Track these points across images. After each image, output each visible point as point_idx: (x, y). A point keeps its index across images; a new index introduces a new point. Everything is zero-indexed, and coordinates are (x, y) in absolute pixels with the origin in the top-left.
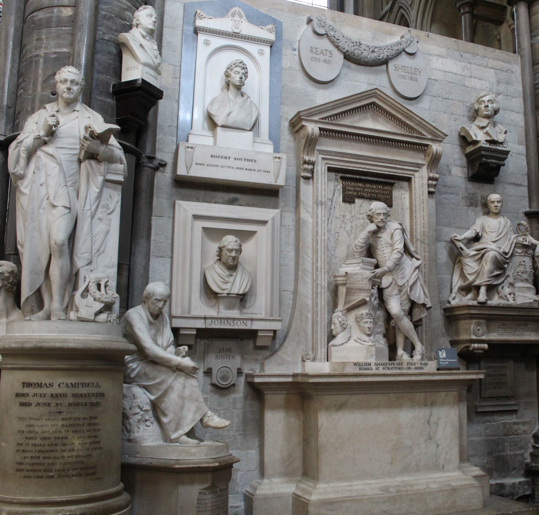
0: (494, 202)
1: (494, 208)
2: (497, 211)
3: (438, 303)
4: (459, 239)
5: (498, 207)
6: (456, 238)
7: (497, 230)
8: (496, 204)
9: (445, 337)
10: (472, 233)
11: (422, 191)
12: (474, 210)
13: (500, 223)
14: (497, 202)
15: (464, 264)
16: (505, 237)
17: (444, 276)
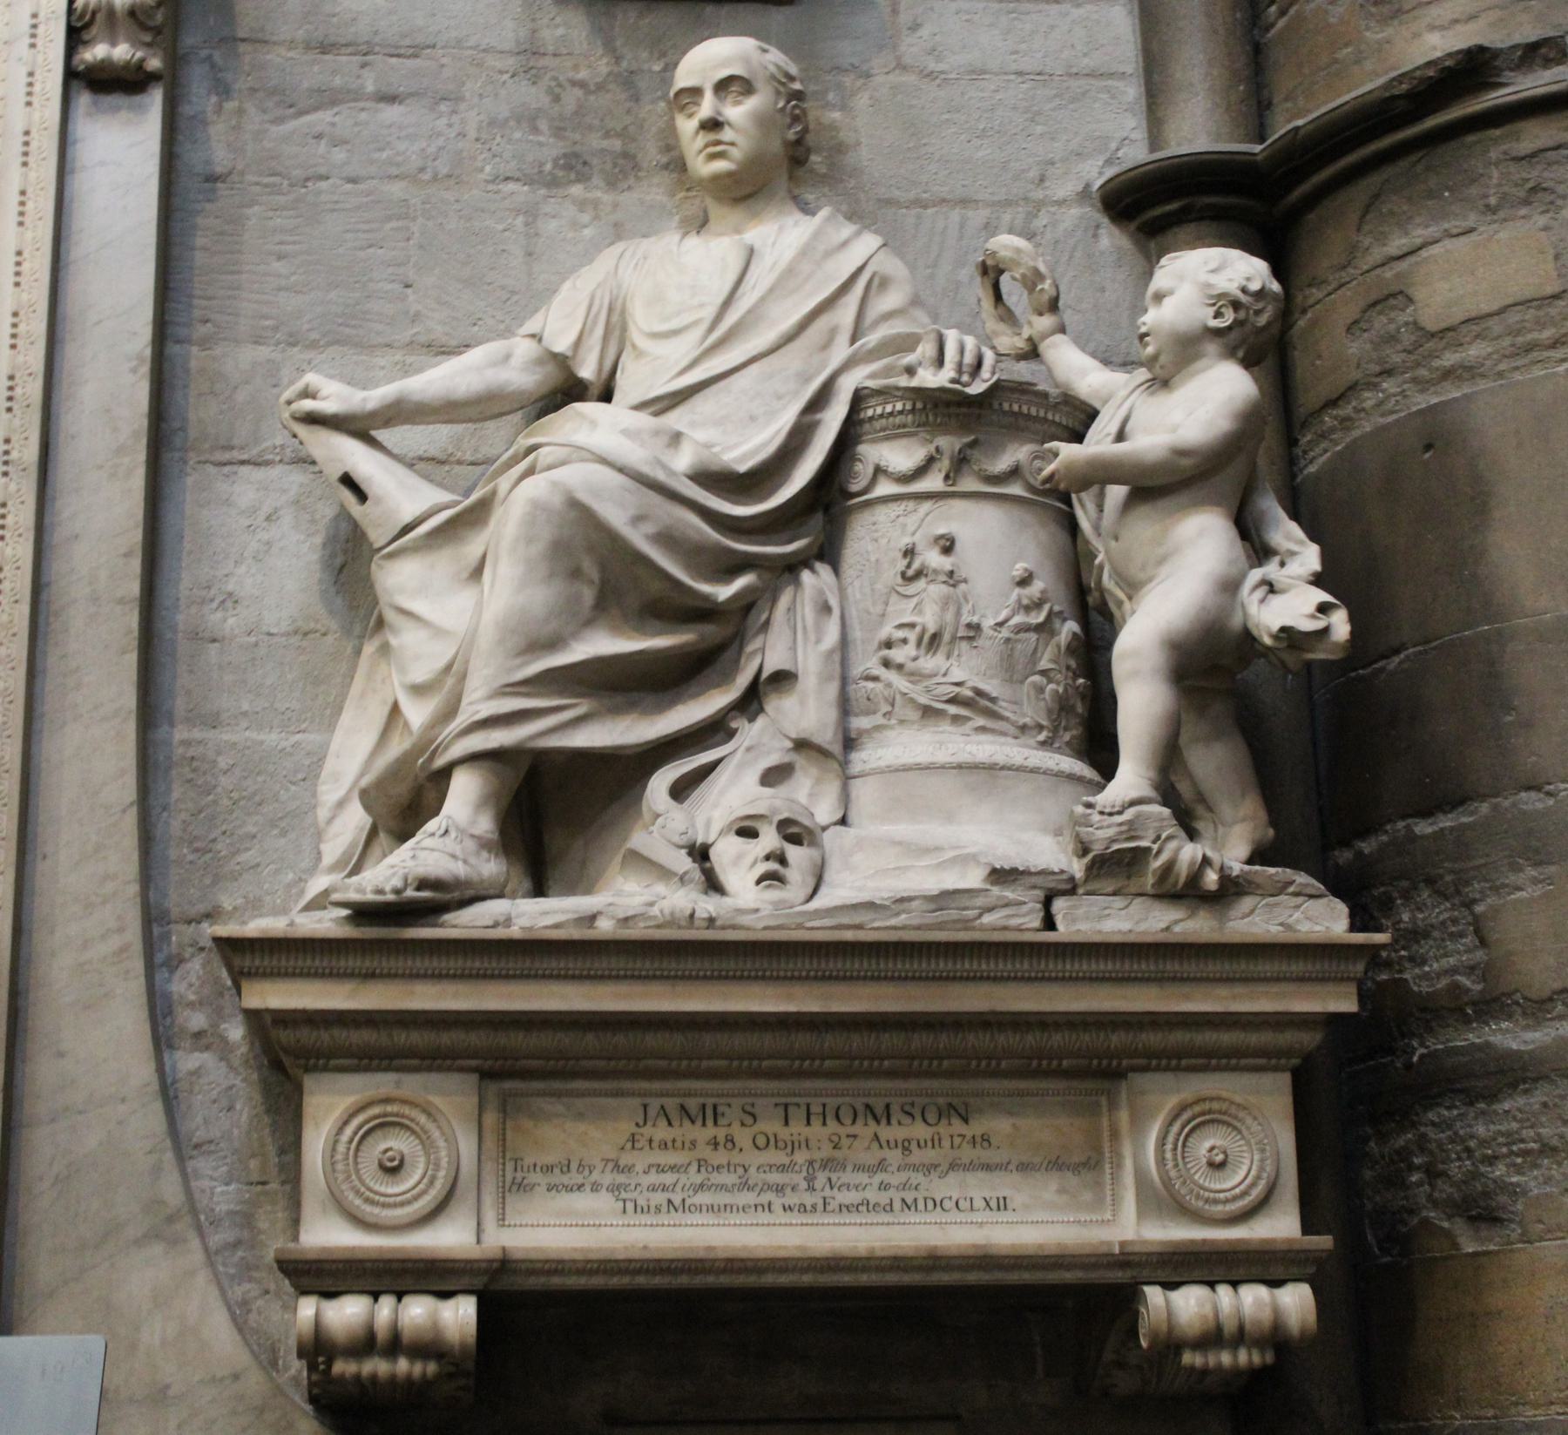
0: (695, 92)
1: (702, 139)
2: (721, 166)
3: (124, 949)
4: (327, 406)
5: (727, 134)
6: (308, 405)
7: (709, 313)
8: (707, 106)
9: (175, 1242)
10: (507, 357)
11: (24, 71)
12: (596, 204)
13: (751, 253)
14: (723, 86)
15: (390, 615)
16: (792, 358)
17: (272, 738)
